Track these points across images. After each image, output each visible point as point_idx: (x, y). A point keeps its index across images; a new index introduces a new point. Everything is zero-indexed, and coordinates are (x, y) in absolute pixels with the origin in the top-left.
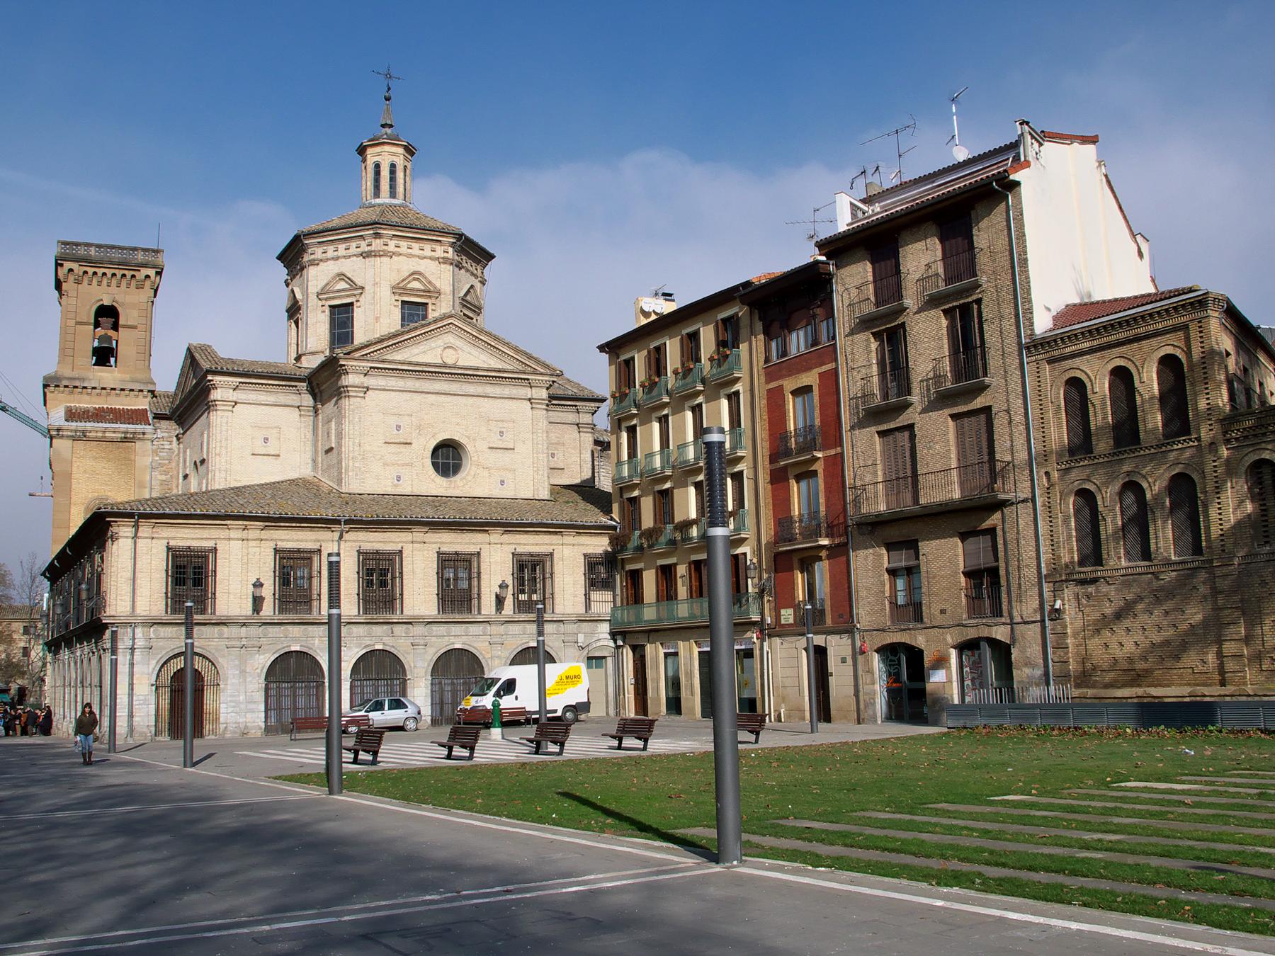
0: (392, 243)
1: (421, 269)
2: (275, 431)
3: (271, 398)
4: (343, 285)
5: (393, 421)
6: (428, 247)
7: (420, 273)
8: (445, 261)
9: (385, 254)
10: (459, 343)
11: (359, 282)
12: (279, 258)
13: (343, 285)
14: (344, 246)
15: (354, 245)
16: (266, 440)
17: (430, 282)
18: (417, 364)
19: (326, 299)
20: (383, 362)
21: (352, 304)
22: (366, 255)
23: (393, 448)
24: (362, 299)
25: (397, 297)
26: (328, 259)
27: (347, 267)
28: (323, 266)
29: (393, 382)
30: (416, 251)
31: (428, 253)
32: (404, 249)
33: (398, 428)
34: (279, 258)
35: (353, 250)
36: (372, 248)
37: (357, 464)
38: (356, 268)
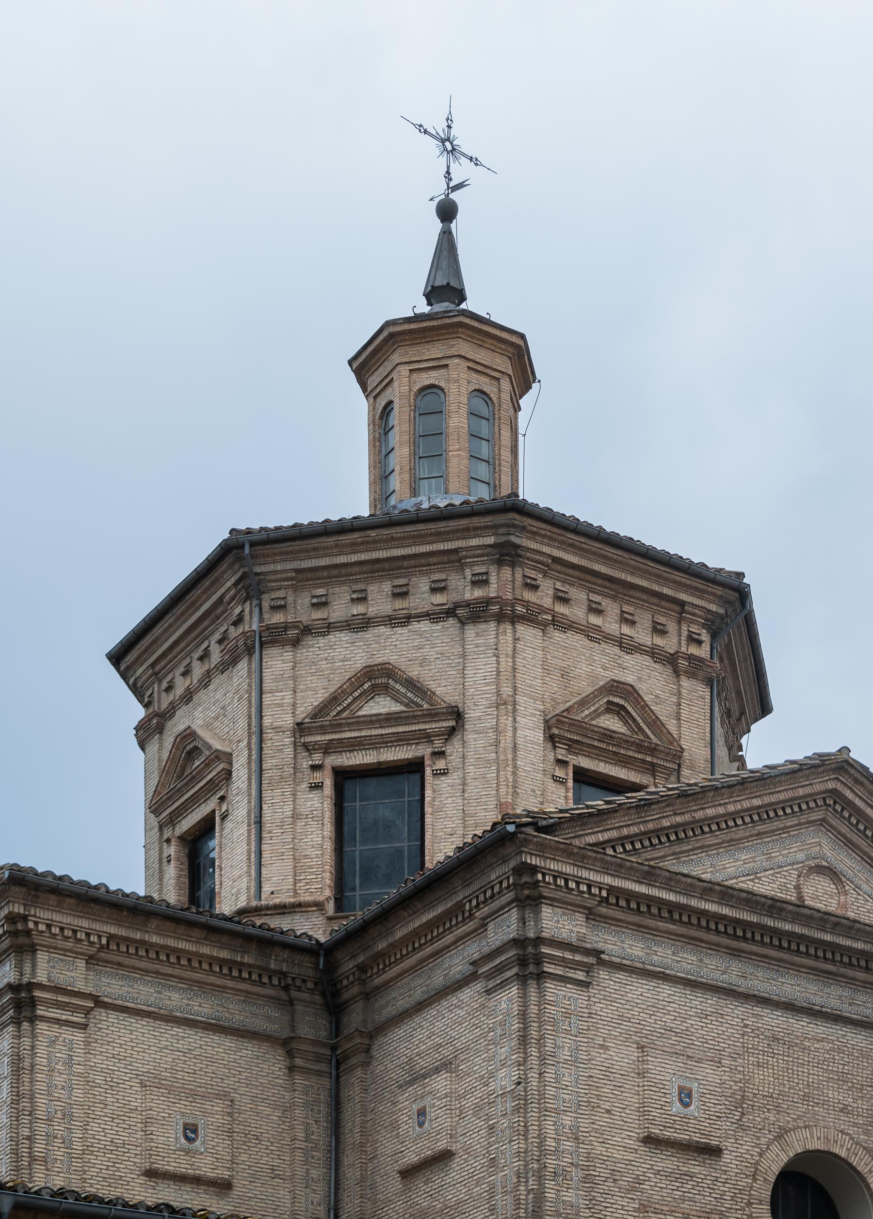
0: (547, 589)
1: (630, 679)
2: (218, 1106)
3: (202, 1007)
4: (382, 706)
5: (667, 1072)
6: (644, 619)
7: (629, 692)
8: (696, 668)
9: (531, 617)
10: (846, 862)
11: (445, 691)
12: (117, 657)
13: (382, 706)
14: (387, 587)
15: (423, 584)
16: (191, 1131)
17: (656, 723)
18: (751, 900)
19: (327, 749)
20: (649, 875)
21: (416, 767)
22: (473, 613)
23: (668, 1162)
24: (454, 749)
25: (561, 753)
26: (329, 628)
27: (394, 647)
28: (315, 648)
29: (664, 955)
30: (611, 625)
31: (643, 636)
32: (577, 612)
33: (685, 1096)
34: (117, 657)
35: (422, 596)
36: (492, 591)
37: (569, 1196)
38: (426, 653)
